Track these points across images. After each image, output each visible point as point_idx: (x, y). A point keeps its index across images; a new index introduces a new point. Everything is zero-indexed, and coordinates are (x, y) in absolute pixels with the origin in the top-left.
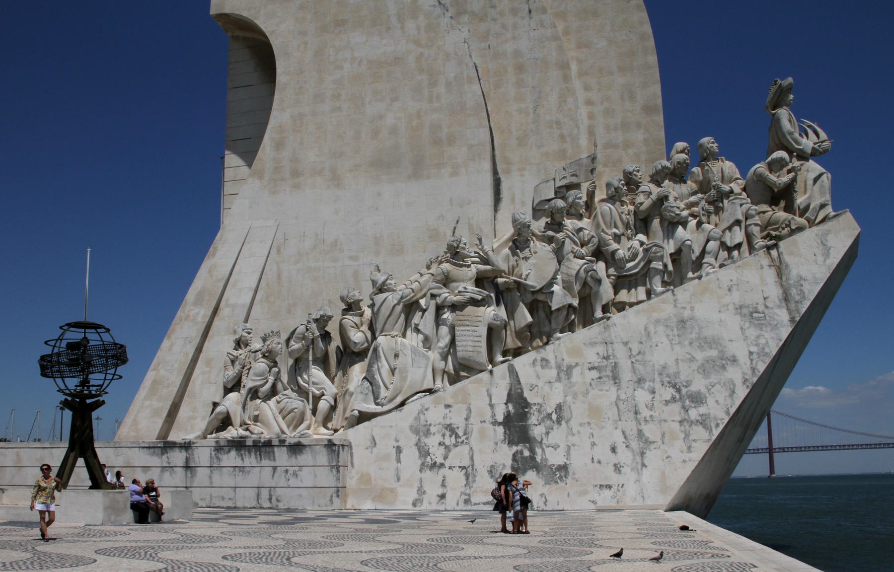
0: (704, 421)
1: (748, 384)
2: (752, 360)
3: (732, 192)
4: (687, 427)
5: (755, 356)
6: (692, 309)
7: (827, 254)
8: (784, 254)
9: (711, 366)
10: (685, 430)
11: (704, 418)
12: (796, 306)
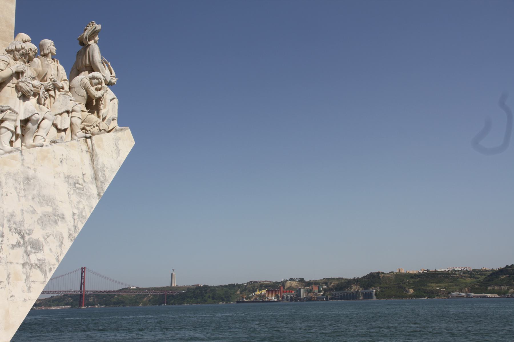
0: (41, 265)
1: (71, 238)
2: (74, 219)
3: (63, 88)
4: (28, 269)
5: (76, 217)
6: (35, 170)
7: (118, 154)
8: (95, 145)
9: (47, 220)
10: (27, 272)
11: (41, 262)
12: (101, 185)
